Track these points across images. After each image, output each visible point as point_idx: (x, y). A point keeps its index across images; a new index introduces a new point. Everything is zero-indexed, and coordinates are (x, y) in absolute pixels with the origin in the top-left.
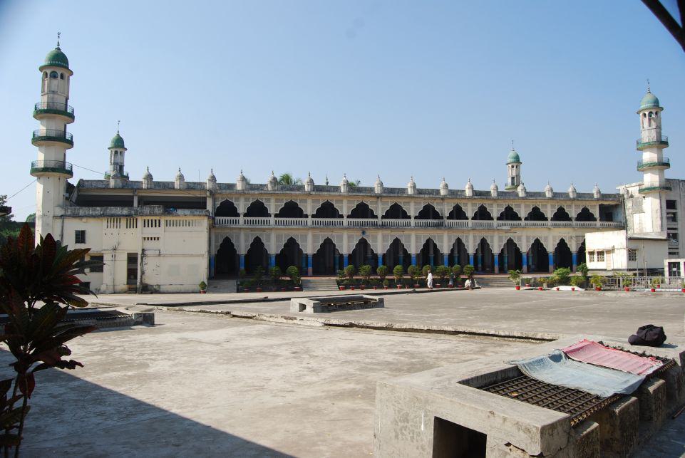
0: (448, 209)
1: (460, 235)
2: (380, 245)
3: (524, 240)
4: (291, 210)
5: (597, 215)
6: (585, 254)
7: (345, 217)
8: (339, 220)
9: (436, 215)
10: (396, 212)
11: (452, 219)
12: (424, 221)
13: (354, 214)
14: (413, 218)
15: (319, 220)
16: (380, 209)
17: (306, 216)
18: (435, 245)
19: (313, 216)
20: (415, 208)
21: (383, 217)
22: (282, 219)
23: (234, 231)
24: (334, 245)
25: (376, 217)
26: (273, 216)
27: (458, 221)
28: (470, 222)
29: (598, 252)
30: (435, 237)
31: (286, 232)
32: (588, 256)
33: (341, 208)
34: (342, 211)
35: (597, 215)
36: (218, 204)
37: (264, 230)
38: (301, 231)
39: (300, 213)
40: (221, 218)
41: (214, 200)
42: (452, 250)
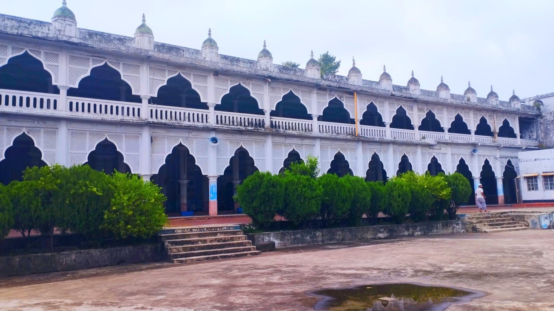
2: (269, 160)
3: (449, 157)
5: (517, 131)
6: (518, 180)
8: (200, 111)
13: (226, 105)
14: (315, 119)
19: (152, 101)
21: (273, 114)
22: (87, 101)
24: (192, 159)
25: (262, 112)
26: (63, 92)
29: (545, 177)
32: (524, 185)
34: (206, 97)
35: (517, 131)
39: (122, 92)
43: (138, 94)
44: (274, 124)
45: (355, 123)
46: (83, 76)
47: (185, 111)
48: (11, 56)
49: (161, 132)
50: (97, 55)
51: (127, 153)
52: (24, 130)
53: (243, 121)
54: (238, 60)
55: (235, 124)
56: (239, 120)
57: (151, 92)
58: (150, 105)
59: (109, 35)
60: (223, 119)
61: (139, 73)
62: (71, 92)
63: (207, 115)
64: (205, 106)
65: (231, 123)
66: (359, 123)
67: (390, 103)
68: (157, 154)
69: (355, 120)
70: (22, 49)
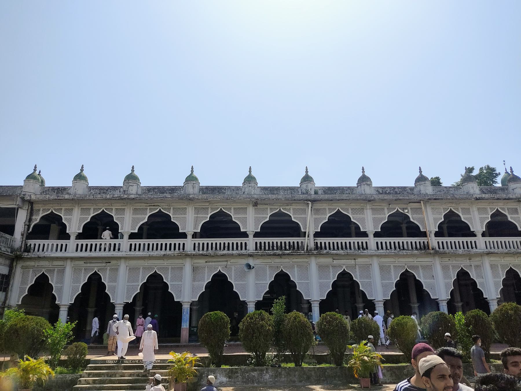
0: (435, 220)
1: (463, 264)
4: (160, 227)
7: (251, 236)
9: (415, 231)
10: (339, 226)
11: (443, 236)
12: (392, 240)
15: (206, 241)
16: (311, 222)
17: (184, 236)
18: (419, 284)
20: (374, 219)
23: (56, 263)
27: (453, 239)
28: (481, 241)
30: (416, 268)
31: (146, 263)
33: (244, 221)
36: (37, 219)
37: (108, 260)
38: (170, 261)
40: (37, 242)
41: (31, 213)
42: (452, 293)
43: (184, 231)
44: (319, 245)
45: (426, 236)
46: (141, 223)
47: (225, 241)
48: (92, 215)
49: (201, 262)
50: (153, 205)
51: (172, 283)
52: (96, 269)
53: (283, 245)
54: (277, 189)
55: (275, 248)
56: (279, 244)
57: (195, 228)
58: (193, 239)
59: (163, 187)
60: (263, 245)
61: (185, 214)
62: (132, 236)
63: (246, 243)
64: (245, 235)
65: (271, 248)
66: (433, 235)
67: (479, 209)
68: (198, 283)
69: (428, 233)
70: (100, 209)
